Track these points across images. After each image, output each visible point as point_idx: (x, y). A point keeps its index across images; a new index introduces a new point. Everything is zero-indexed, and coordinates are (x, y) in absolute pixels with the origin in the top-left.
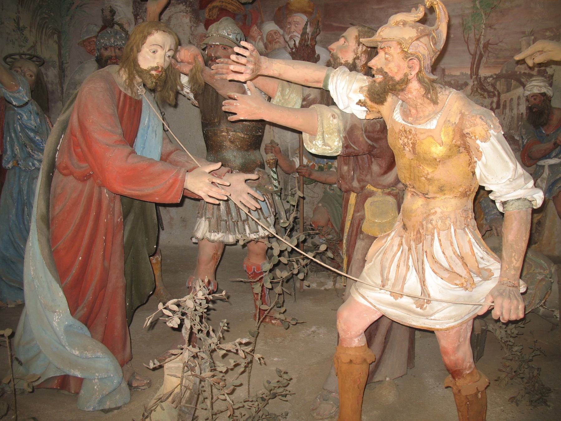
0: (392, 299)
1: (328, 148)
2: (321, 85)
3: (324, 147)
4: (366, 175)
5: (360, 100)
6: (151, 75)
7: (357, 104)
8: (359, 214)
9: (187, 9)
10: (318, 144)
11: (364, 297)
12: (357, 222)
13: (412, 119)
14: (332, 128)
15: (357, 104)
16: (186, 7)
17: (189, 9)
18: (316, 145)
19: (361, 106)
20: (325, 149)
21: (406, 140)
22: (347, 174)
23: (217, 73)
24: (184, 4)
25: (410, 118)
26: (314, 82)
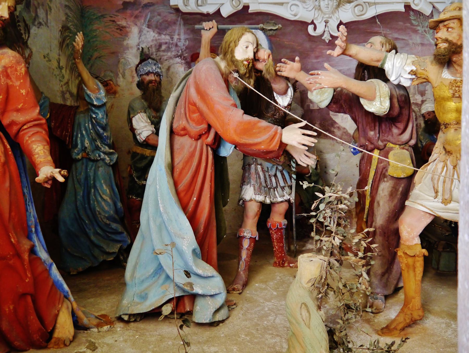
0: (442, 206)
1: (383, 107)
2: (379, 64)
3: (381, 106)
4: (388, 136)
5: (412, 71)
6: (244, 65)
7: (409, 73)
8: (382, 165)
9: (182, 61)
10: (377, 104)
11: (422, 205)
12: (381, 170)
13: (459, 75)
14: (385, 93)
15: (409, 73)
16: (181, 60)
17: (183, 61)
18: (375, 104)
19: (412, 75)
20: (381, 108)
21: (457, 89)
22: (374, 136)
23: (279, 71)
24: (179, 57)
25: (457, 75)
26: (376, 61)
